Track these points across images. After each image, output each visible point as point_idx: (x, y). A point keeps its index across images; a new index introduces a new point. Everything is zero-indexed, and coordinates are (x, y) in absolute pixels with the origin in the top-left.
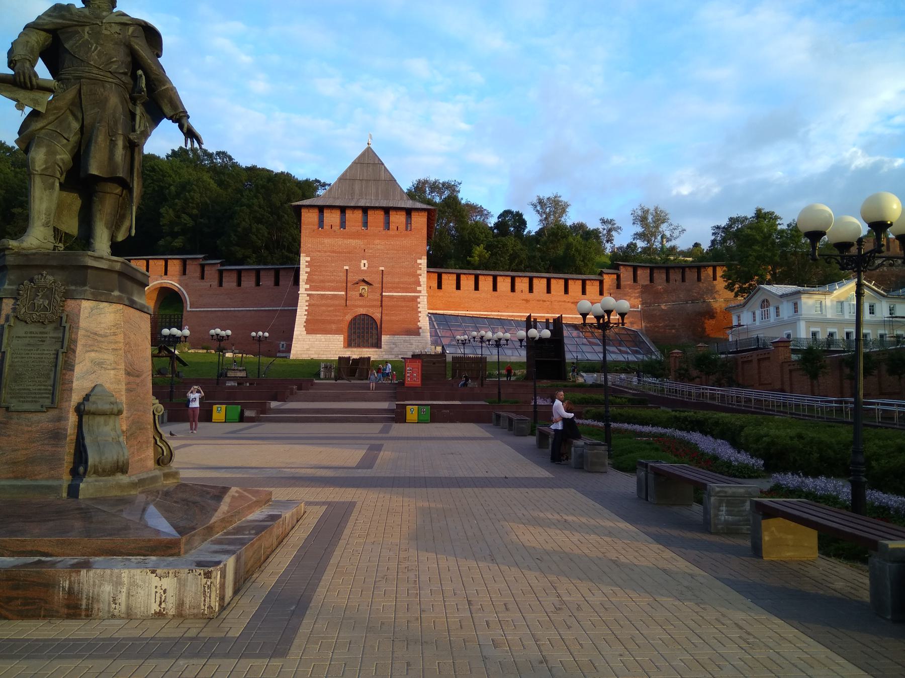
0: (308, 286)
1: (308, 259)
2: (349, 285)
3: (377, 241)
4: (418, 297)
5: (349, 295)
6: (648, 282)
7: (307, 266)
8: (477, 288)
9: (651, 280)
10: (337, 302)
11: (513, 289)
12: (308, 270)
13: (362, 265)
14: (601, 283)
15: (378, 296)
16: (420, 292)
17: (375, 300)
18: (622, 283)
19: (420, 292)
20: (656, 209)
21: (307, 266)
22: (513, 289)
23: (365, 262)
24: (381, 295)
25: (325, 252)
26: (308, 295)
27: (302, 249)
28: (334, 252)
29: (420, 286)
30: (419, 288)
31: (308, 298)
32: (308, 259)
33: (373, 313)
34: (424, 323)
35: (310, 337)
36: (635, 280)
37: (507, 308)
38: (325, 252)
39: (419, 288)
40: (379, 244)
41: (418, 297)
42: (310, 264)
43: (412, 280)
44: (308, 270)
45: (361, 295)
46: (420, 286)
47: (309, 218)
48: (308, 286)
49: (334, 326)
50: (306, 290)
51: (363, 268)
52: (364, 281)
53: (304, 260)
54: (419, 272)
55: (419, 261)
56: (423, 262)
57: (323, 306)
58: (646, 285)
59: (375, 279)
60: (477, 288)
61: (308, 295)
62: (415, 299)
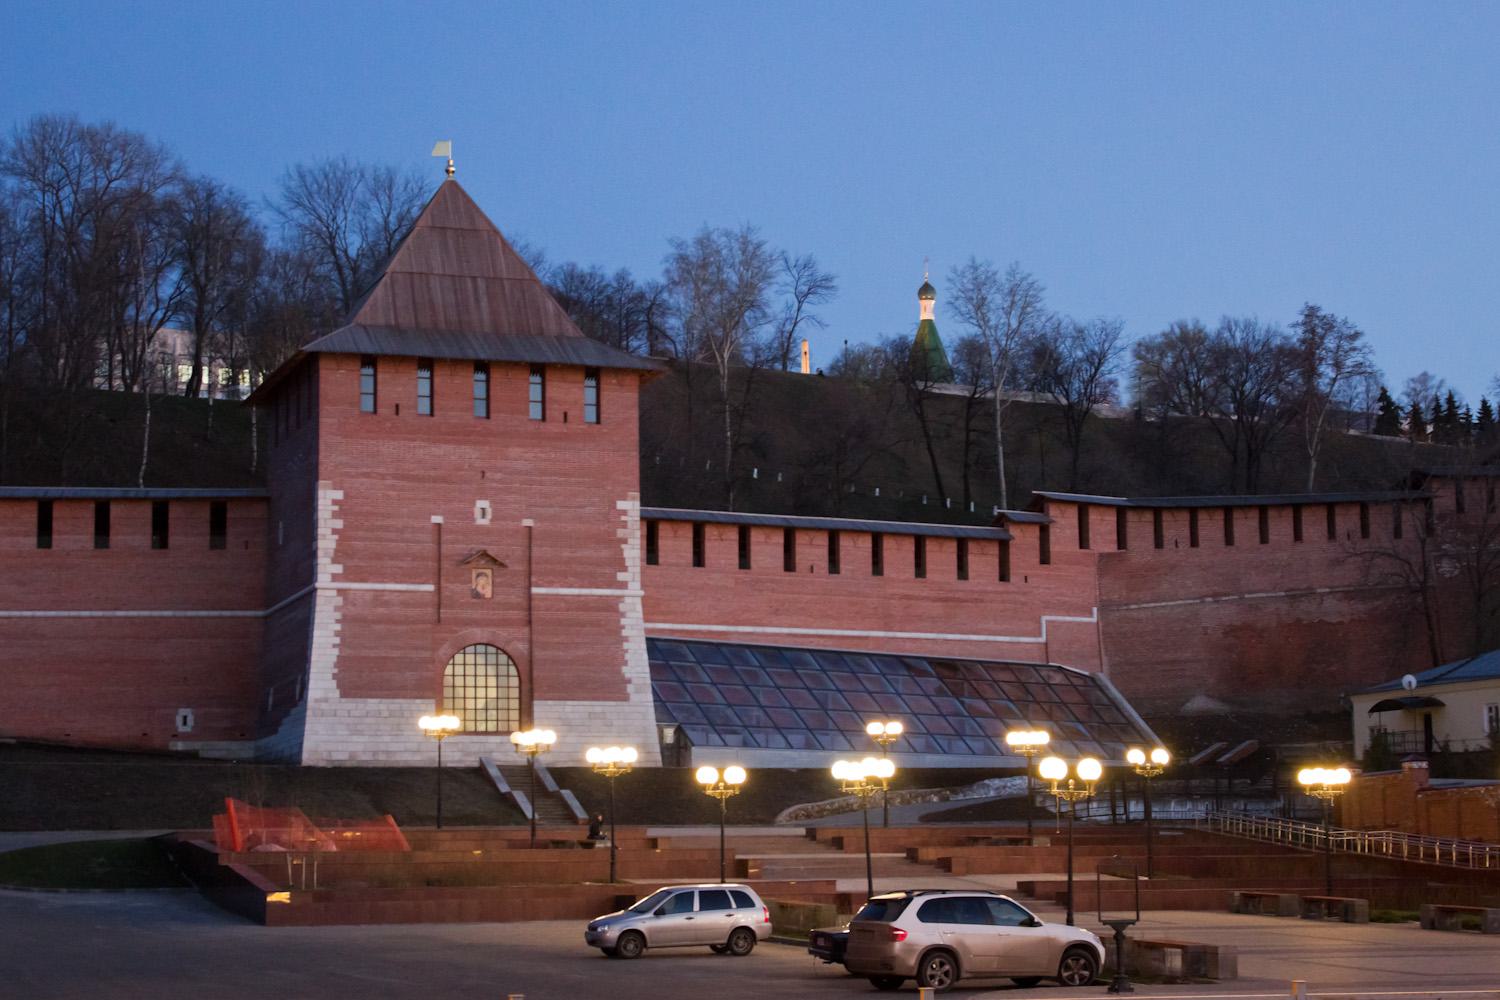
0: (338, 569)
1: (339, 495)
2: (445, 565)
3: (514, 452)
4: (620, 598)
5: (445, 593)
6: (1113, 548)
7: (335, 515)
8: (699, 560)
9: (1122, 542)
10: (412, 612)
11: (789, 565)
12: (339, 524)
13: (477, 513)
14: (1004, 545)
15: (516, 597)
16: (623, 585)
17: (512, 607)
18: (1054, 548)
19: (623, 585)
20: (1012, 273)
21: (335, 515)
22: (789, 565)
23: (481, 504)
24: (530, 597)
25: (383, 477)
26: (340, 592)
27: (322, 469)
28: (404, 477)
29: (624, 569)
30: (621, 576)
31: (340, 601)
32: (339, 495)
33: (508, 642)
34: (637, 665)
35: (349, 704)
36: (1083, 542)
37: (777, 613)
38: (383, 477)
39: (621, 576)
40: (520, 457)
41: (620, 598)
42: (343, 510)
43: (605, 553)
44: (339, 524)
45: (477, 595)
46: (624, 569)
47: (337, 386)
48: (338, 569)
49: (410, 676)
50: (335, 577)
51: (480, 521)
52: (485, 554)
53: (327, 498)
54: (620, 533)
55: (621, 505)
56: (631, 507)
57: (379, 621)
58: (1109, 555)
59: (511, 551)
60: (699, 560)
61: (340, 592)
62: (611, 607)
